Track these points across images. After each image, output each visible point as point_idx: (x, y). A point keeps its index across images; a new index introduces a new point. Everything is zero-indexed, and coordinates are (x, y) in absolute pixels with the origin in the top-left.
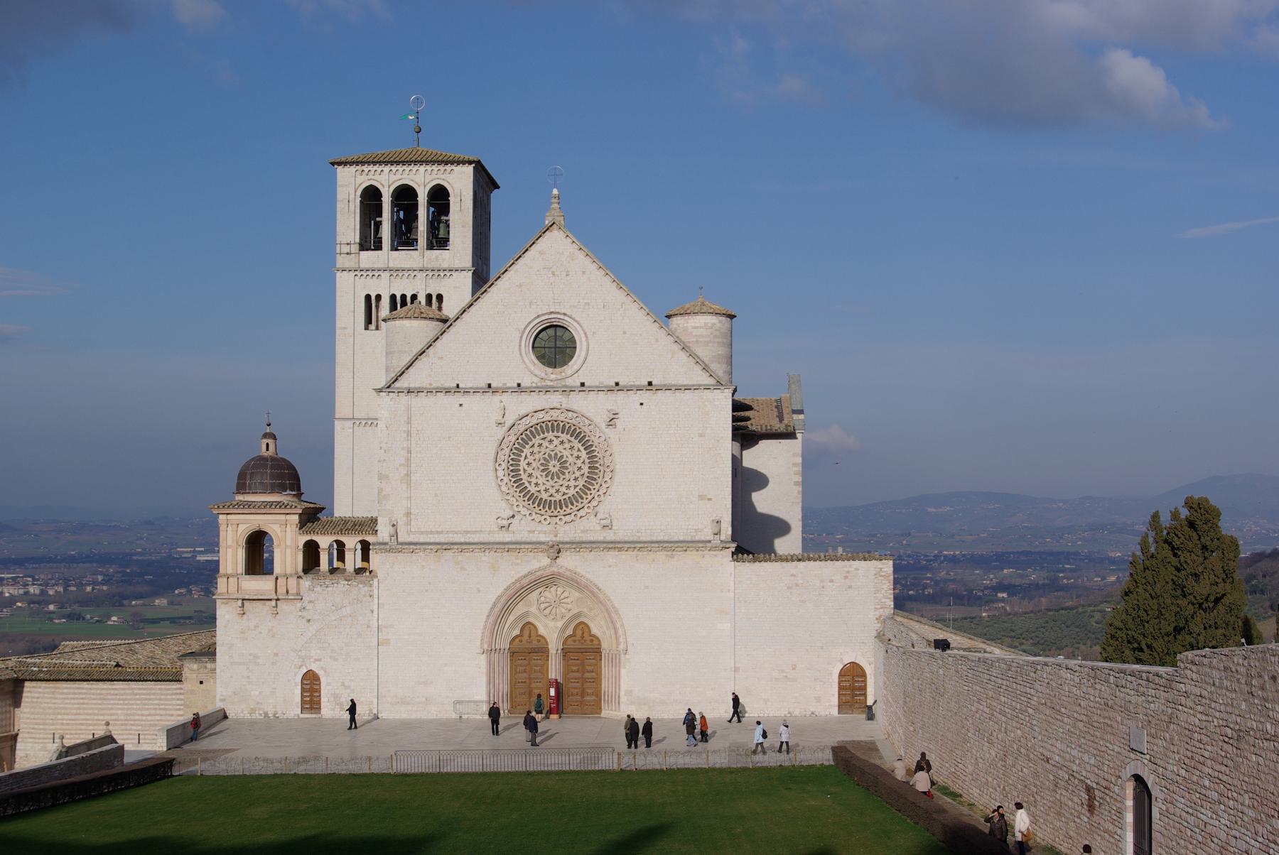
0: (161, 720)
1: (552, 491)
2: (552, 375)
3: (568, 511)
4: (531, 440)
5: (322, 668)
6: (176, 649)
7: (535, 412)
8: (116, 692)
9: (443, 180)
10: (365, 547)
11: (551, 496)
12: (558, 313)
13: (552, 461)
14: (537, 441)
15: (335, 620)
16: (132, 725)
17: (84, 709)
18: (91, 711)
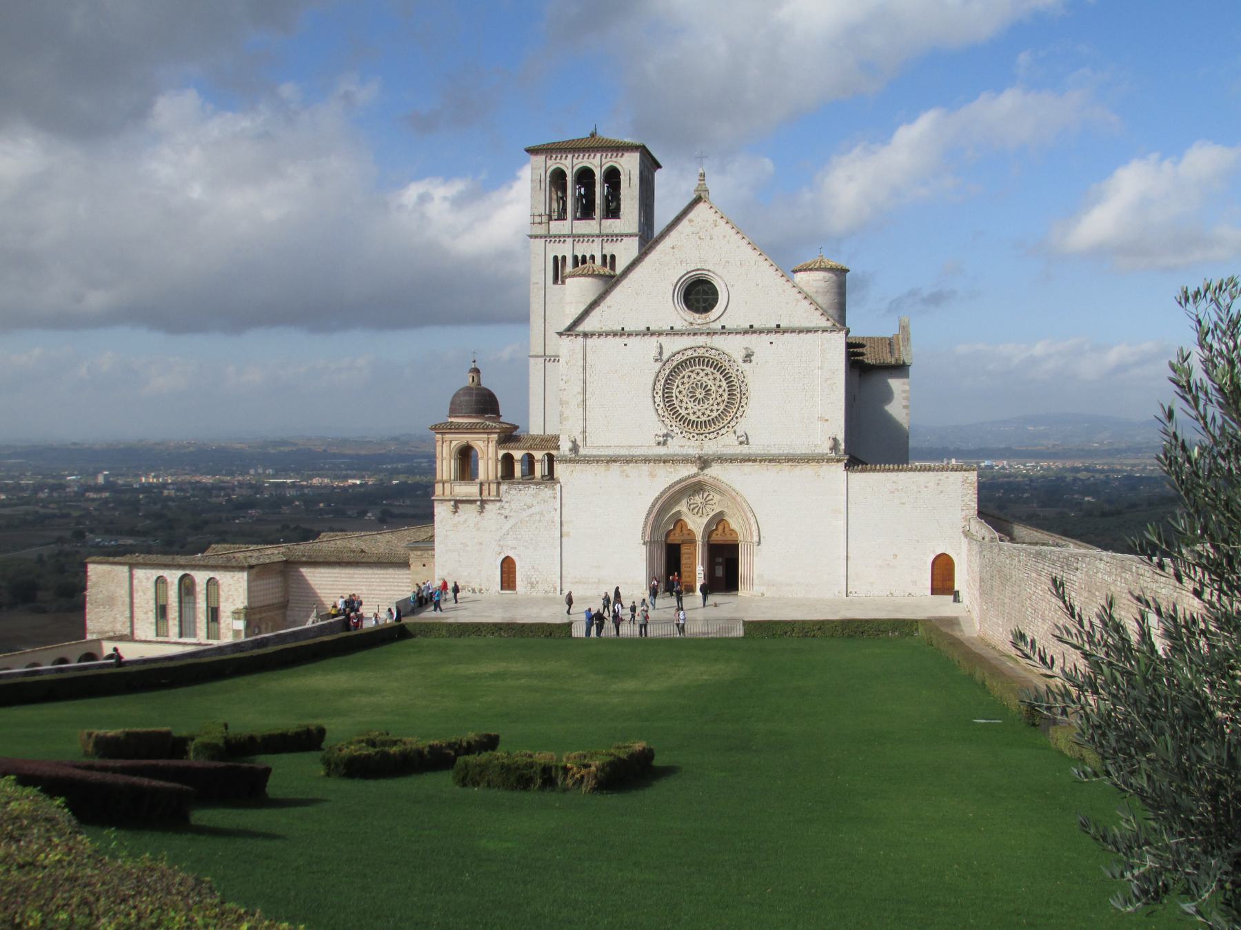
1: (699, 414)
2: (698, 319)
3: (712, 430)
4: (682, 373)
5: (517, 554)
6: (409, 538)
7: (686, 350)
9: (616, 162)
10: (551, 458)
11: (698, 417)
12: (704, 270)
13: (698, 389)
14: (686, 373)
15: (527, 517)
16: (373, 598)
17: (339, 585)
18: (341, 587)
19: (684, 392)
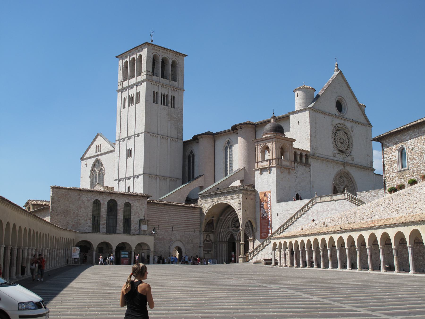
0: (179, 222)
8: (166, 210)
14: (338, 132)
16: (171, 223)
17: (156, 216)
18: (157, 217)
19: (338, 139)
